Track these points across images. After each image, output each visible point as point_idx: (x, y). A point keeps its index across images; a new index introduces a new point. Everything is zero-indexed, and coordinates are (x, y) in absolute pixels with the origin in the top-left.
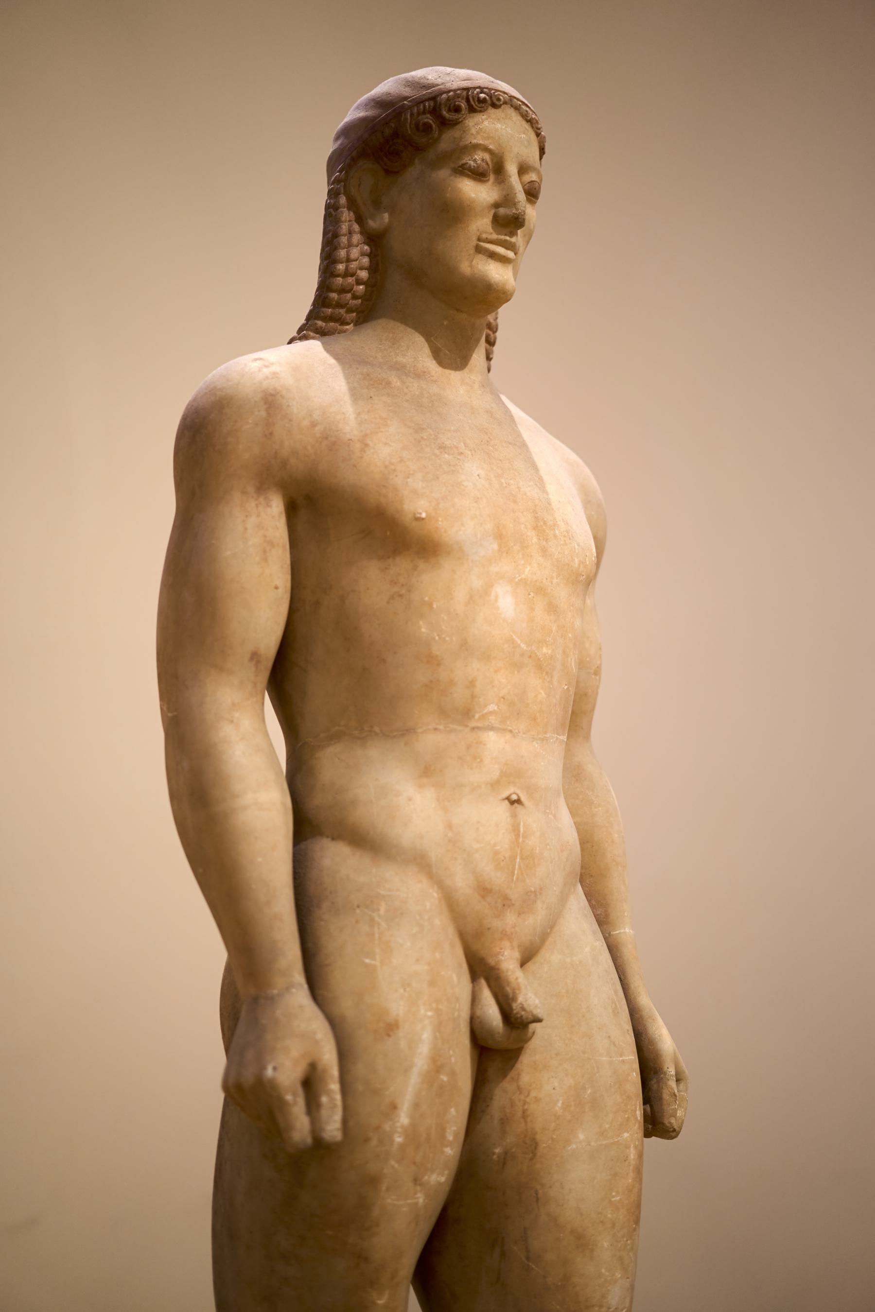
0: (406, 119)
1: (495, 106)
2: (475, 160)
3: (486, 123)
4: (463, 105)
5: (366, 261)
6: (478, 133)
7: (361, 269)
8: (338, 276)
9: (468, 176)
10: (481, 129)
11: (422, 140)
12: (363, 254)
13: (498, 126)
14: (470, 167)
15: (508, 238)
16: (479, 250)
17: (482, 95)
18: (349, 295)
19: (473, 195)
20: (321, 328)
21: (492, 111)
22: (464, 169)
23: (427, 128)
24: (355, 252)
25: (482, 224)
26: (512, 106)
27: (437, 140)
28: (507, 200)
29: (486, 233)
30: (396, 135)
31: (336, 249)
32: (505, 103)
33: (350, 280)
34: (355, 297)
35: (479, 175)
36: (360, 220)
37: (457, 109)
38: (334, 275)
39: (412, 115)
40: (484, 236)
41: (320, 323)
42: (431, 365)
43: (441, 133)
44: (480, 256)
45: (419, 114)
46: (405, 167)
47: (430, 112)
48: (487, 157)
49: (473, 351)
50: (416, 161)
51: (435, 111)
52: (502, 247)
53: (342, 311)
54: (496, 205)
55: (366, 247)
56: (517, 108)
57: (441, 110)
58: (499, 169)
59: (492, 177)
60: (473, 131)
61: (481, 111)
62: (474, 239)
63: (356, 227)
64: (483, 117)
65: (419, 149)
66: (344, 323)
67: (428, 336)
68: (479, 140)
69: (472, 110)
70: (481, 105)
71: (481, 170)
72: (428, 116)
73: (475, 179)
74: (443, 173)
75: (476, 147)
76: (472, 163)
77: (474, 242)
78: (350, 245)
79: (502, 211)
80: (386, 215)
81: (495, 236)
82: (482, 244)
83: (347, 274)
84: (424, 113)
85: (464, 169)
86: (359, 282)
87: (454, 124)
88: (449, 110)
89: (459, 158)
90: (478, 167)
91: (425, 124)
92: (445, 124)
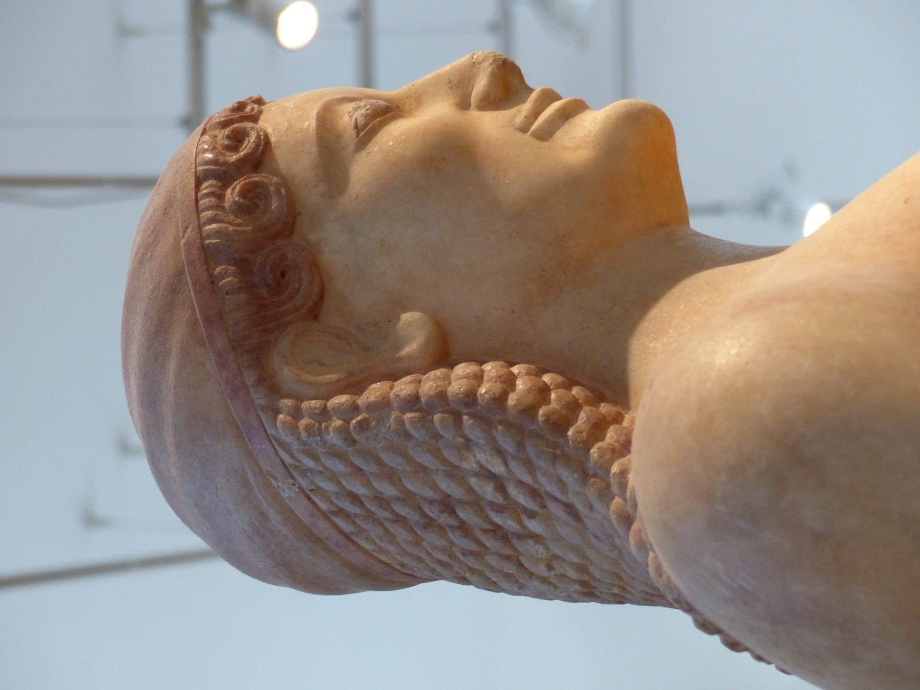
0: (218, 233)
8: (504, 396)
14: (367, 115)
16: (546, 134)
22: (366, 125)
23: (254, 198)
25: (491, 125)
27: (285, 183)
29: (514, 116)
30: (243, 265)
31: (442, 396)
36: (394, 377)
38: (500, 399)
39: (213, 220)
43: (277, 173)
44: (559, 134)
45: (219, 207)
46: (315, 266)
47: (225, 187)
50: (312, 237)
54: (464, 105)
57: (225, 163)
62: (518, 134)
65: (289, 224)
66: (617, 419)
72: (229, 191)
74: (364, 168)
80: (406, 317)
82: (533, 128)
83: (510, 382)
84: (221, 197)
87: (265, 144)
88: (234, 148)
89: (339, 136)
91: (243, 194)
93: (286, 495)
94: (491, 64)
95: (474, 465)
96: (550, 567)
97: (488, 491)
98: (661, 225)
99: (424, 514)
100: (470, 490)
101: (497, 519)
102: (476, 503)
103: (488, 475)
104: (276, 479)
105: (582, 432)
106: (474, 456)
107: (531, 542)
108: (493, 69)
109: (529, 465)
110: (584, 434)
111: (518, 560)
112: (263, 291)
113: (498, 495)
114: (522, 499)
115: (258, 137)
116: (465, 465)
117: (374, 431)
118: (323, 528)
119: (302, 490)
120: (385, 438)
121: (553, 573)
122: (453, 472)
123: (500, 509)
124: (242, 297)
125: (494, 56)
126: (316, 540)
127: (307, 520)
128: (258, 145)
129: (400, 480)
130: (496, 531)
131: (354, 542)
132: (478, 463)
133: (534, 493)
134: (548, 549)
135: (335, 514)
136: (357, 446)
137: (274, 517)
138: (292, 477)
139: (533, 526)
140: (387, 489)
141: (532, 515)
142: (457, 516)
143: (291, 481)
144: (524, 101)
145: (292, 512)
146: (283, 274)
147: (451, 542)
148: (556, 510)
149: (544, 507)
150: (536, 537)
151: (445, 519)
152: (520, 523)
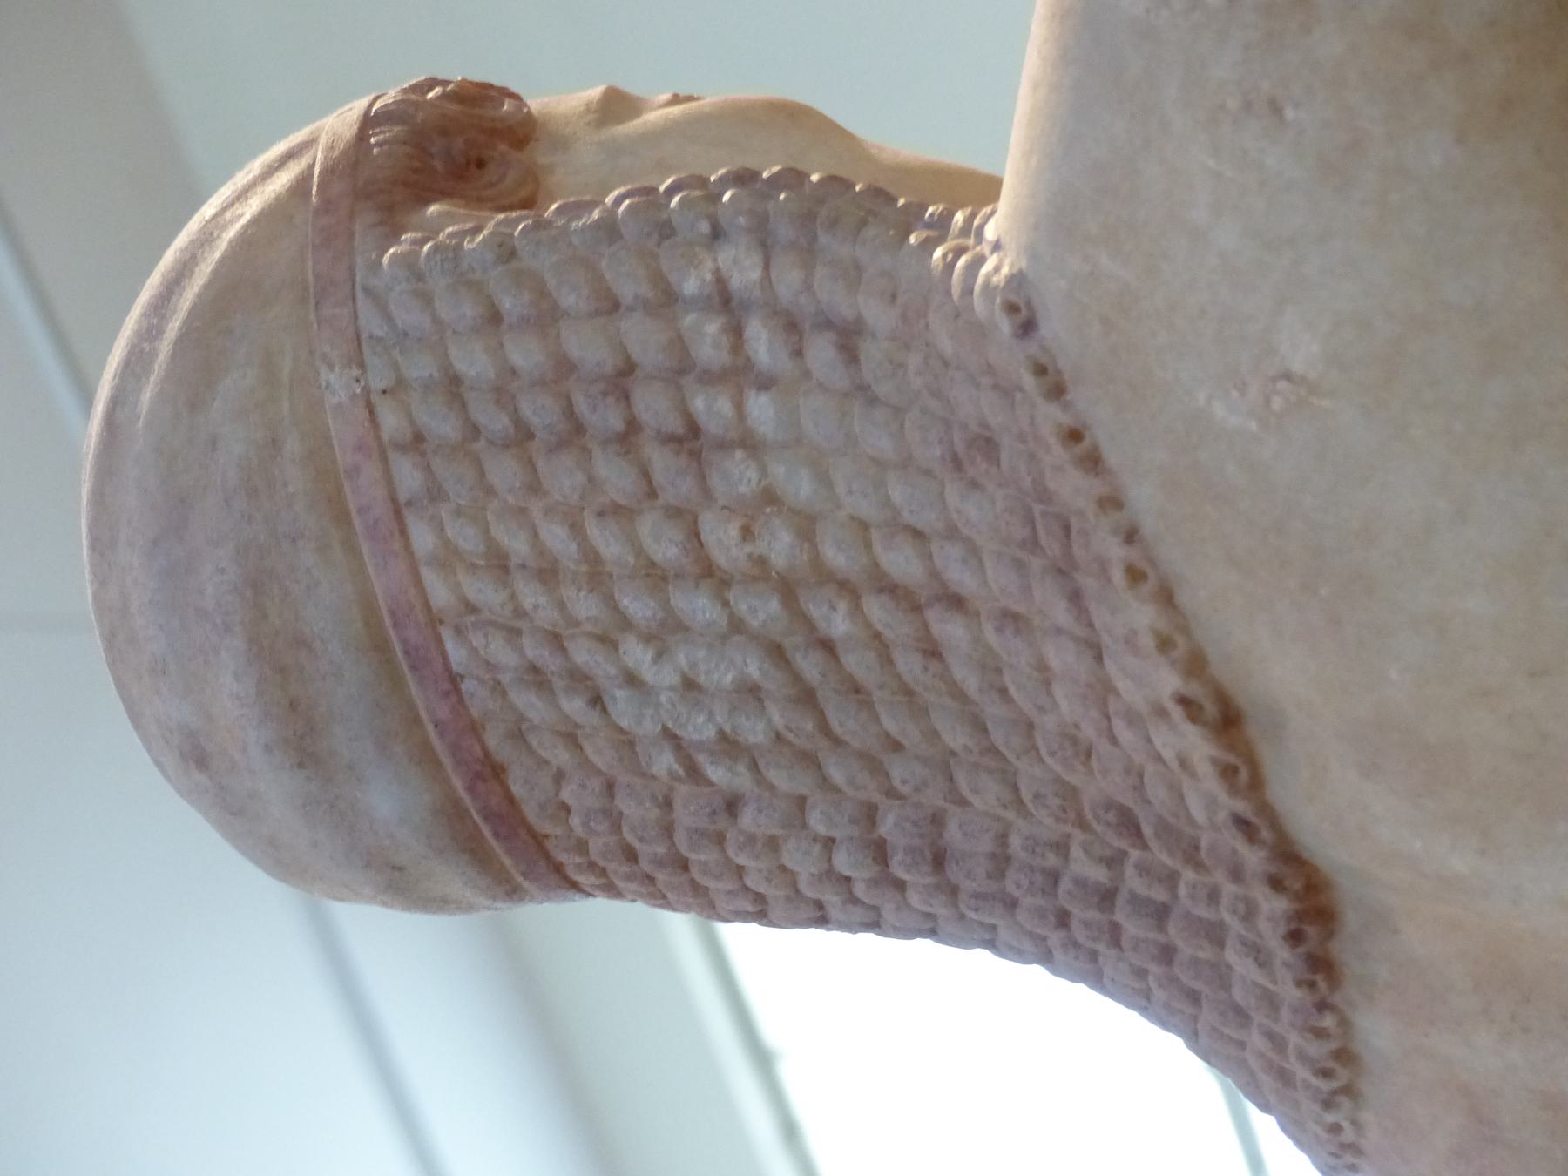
50: (543, 160)
93: (335, 401)
95: (708, 277)
96: (747, 533)
97: (708, 337)
99: (569, 411)
100: (679, 345)
101: (699, 404)
102: (681, 368)
103: (724, 300)
104: (331, 367)
106: (715, 260)
107: (739, 454)
109: (808, 254)
111: (696, 522)
112: (438, 165)
113: (724, 338)
114: (762, 343)
116: (690, 286)
117: (554, 232)
118: (365, 491)
119: (367, 391)
120: (570, 243)
121: (748, 548)
122: (666, 300)
123: (710, 378)
124: (408, 149)
126: (342, 517)
127: (344, 458)
129: (558, 336)
130: (689, 439)
131: (403, 532)
132: (717, 272)
133: (791, 326)
134: (763, 471)
135: (402, 448)
136: (514, 264)
137: (293, 445)
138: (362, 366)
139: (761, 409)
140: (525, 354)
141: (766, 383)
142: (629, 406)
143: (356, 372)
145: (328, 439)
146: (481, 164)
147: (591, 479)
148: (821, 352)
149: (798, 353)
150: (750, 444)
151: (606, 417)
152: (739, 407)
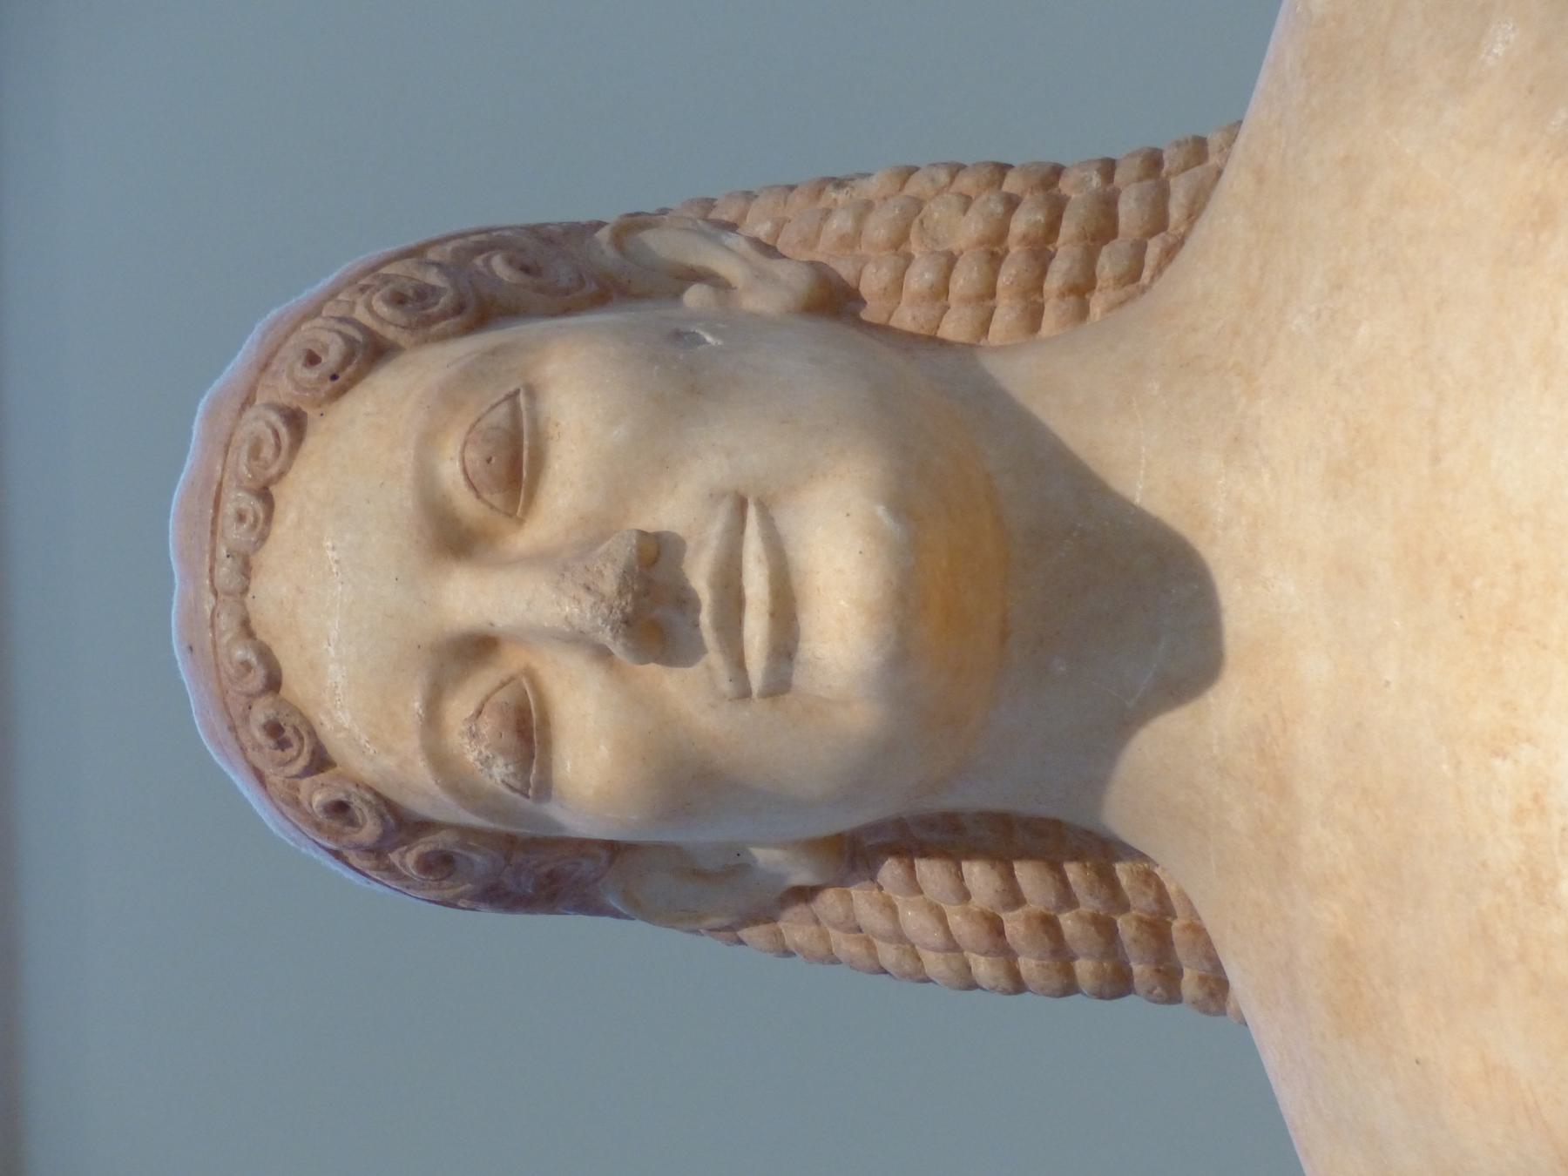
1: (274, 683)
2: (486, 762)
3: (345, 718)
4: (317, 795)
5: (930, 872)
6: (389, 751)
7: (965, 896)
9: (546, 768)
10: (373, 739)
11: (480, 861)
12: (914, 886)
13: (336, 674)
15: (705, 619)
16: (779, 685)
17: (259, 736)
18: (1067, 921)
19: (604, 752)
20: (1203, 980)
21: (297, 685)
24: (914, 920)
26: (245, 590)
27: (465, 832)
28: (576, 639)
32: (246, 629)
33: (1015, 925)
34: (1067, 898)
35: (528, 731)
36: (804, 894)
37: (340, 809)
40: (726, 686)
41: (1189, 984)
42: (1226, 708)
44: (798, 679)
48: (459, 708)
49: (1123, 506)
51: (377, 852)
52: (740, 622)
53: (1126, 927)
54: (602, 654)
55: (890, 870)
56: (246, 569)
58: (477, 647)
59: (512, 660)
60: (389, 762)
61: (313, 733)
63: (829, 901)
64: (329, 726)
67: (1124, 722)
68: (411, 745)
69: (321, 761)
70: (289, 733)
71: (509, 739)
73: (547, 744)
75: (440, 761)
76: (499, 773)
77: (758, 705)
78: (899, 937)
79: (617, 649)
81: (714, 657)
85: (528, 785)
86: (1015, 898)
88: (352, 822)
90: (503, 752)
92: (401, 825)
94: (615, 638)
98: (1004, 637)
105: (1154, 988)
108: (624, 645)
110: (1158, 990)
115: (367, 803)
125: (605, 621)
128: (382, 817)
144: (697, 650)
